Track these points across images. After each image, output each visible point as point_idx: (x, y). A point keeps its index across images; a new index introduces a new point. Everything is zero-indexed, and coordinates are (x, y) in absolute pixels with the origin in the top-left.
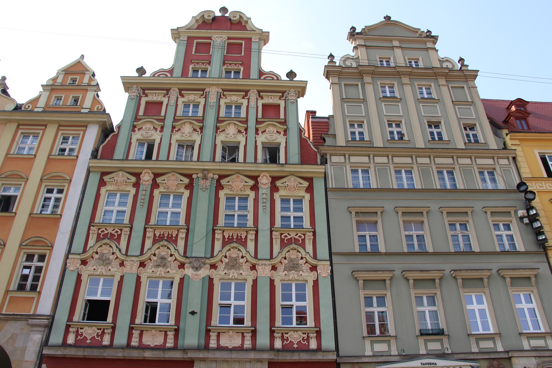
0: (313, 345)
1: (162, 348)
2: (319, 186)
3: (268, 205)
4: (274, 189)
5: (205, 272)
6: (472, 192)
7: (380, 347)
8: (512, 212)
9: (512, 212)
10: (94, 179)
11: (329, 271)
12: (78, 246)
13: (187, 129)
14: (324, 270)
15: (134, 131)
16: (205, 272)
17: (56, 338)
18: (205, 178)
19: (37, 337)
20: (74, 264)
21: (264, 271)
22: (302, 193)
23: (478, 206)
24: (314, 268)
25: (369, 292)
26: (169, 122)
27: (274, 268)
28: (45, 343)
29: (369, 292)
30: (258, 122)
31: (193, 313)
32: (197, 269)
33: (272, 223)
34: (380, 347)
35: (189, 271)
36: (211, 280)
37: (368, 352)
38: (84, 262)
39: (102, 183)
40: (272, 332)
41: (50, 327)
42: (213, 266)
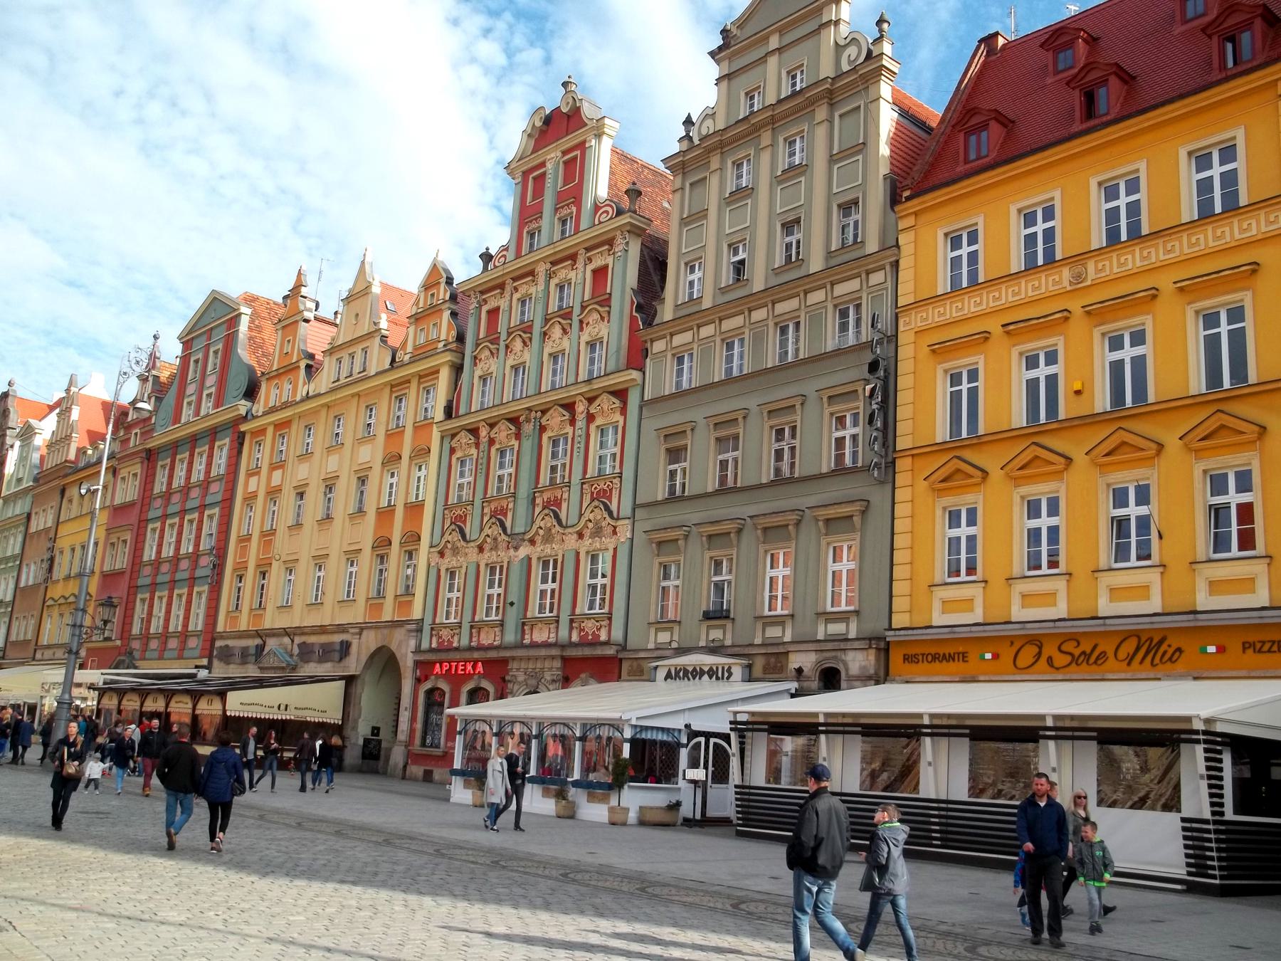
0: (603, 637)
2: (633, 399)
3: (582, 445)
4: (590, 418)
5: (524, 551)
6: (819, 360)
8: (860, 391)
9: (860, 391)
11: (629, 535)
14: (625, 531)
15: (475, 365)
18: (528, 421)
19: (412, 643)
21: (571, 542)
22: (618, 417)
23: (809, 388)
24: (615, 533)
25: (664, 559)
27: (580, 535)
28: (418, 650)
29: (664, 559)
30: (583, 308)
31: (512, 604)
32: (516, 548)
33: (585, 472)
34: (664, 637)
35: (512, 552)
36: (530, 559)
37: (651, 646)
38: (442, 554)
39: (452, 451)
40: (572, 621)
41: (420, 630)
42: (532, 542)
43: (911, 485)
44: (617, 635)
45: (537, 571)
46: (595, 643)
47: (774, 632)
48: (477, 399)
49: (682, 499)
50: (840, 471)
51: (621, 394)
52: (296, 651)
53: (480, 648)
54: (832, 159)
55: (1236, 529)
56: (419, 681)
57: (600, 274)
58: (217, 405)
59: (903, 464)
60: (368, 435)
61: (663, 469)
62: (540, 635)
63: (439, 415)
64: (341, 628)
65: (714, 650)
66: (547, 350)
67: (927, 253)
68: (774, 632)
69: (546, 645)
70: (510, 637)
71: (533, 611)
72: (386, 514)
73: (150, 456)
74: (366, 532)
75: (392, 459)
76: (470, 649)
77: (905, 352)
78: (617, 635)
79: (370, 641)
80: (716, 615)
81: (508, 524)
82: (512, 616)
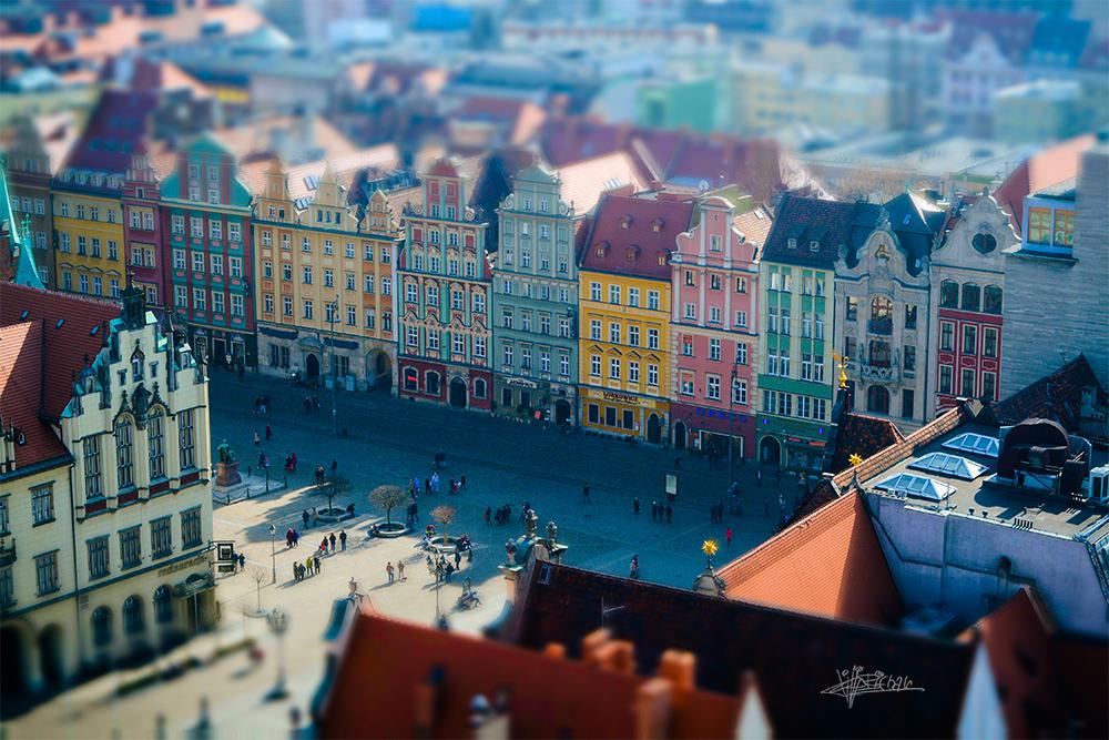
0: (485, 364)
1: (434, 359)
2: (489, 290)
4: (471, 291)
5: (447, 329)
7: (508, 370)
10: (401, 277)
12: (401, 314)
13: (434, 251)
16: (447, 329)
17: (402, 352)
19: (395, 350)
20: (402, 322)
21: (468, 331)
26: (425, 245)
28: (398, 354)
36: (449, 333)
43: (583, 347)
44: (490, 365)
45: (453, 337)
46: (481, 366)
47: (545, 376)
48: (411, 264)
49: (509, 328)
50: (562, 337)
51: (484, 288)
52: (322, 341)
53: (430, 358)
54: (557, 242)
55: (653, 379)
56: (400, 366)
57: (469, 239)
58: (226, 198)
59: (581, 341)
60: (350, 257)
61: (503, 317)
62: (458, 359)
63: (394, 265)
64: (351, 336)
65: (527, 378)
66: (448, 257)
67: (588, 280)
68: (545, 376)
69: (460, 364)
70: (445, 357)
71: (453, 350)
72: (369, 294)
73: (165, 214)
74: (357, 299)
75: (369, 274)
76: (425, 358)
77: (581, 311)
78: (490, 365)
79: (370, 345)
80: (525, 367)
81: (438, 316)
82: (444, 351)
